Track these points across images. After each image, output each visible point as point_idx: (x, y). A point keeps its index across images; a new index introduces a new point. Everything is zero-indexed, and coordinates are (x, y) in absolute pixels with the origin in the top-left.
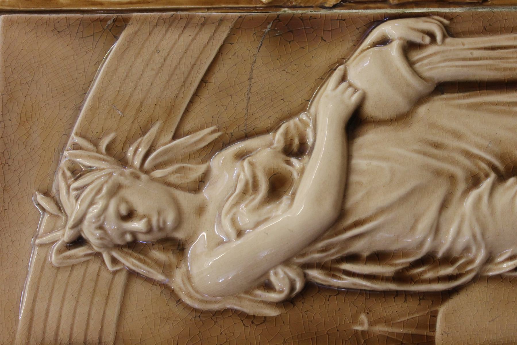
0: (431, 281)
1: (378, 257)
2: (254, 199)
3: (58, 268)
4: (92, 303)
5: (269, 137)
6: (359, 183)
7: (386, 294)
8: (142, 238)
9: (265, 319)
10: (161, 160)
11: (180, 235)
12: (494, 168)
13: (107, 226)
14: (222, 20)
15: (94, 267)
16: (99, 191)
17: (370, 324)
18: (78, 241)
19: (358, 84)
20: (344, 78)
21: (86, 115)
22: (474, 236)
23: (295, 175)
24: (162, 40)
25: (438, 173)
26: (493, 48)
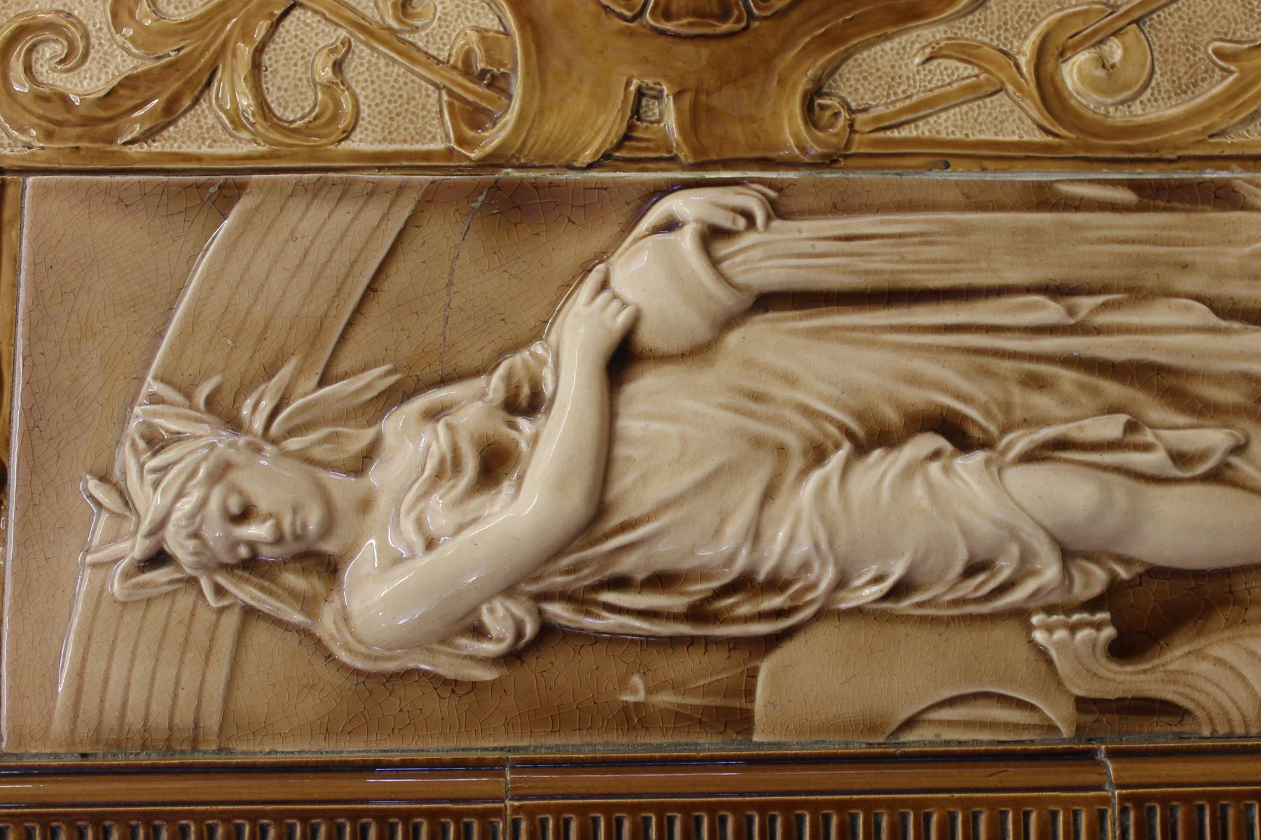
0: (747, 619)
1: (661, 581)
2: (453, 486)
3: (125, 604)
4: (182, 661)
5: (481, 382)
6: (629, 459)
7: (674, 642)
8: (267, 553)
9: (474, 685)
10: (298, 421)
11: (330, 547)
12: (849, 434)
13: (206, 533)
14: (402, 188)
15: (185, 601)
16: (193, 473)
17: (649, 691)
18: (158, 558)
19: (628, 294)
20: (604, 285)
21: (171, 345)
22: (817, 546)
23: (523, 446)
24: (301, 220)
25: (758, 442)
26: (848, 238)
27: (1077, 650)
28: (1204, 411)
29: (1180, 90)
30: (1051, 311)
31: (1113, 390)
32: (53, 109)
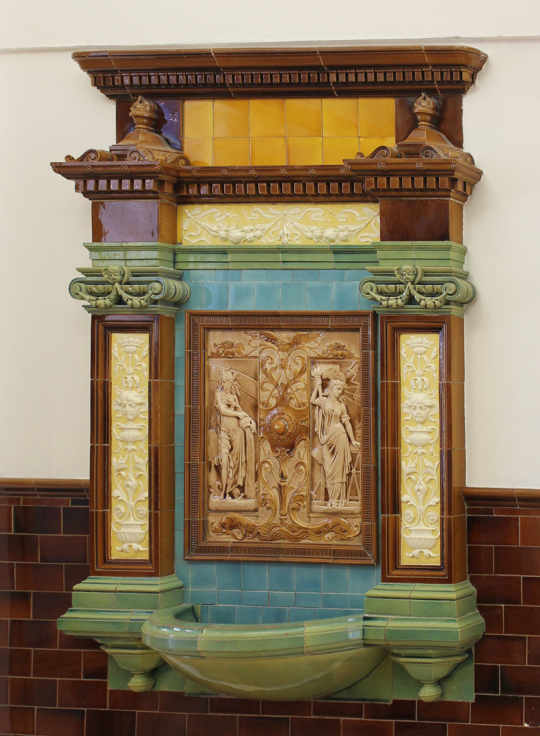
27: (215, 462)
29: (265, 476)
30: (244, 461)
31: (237, 467)
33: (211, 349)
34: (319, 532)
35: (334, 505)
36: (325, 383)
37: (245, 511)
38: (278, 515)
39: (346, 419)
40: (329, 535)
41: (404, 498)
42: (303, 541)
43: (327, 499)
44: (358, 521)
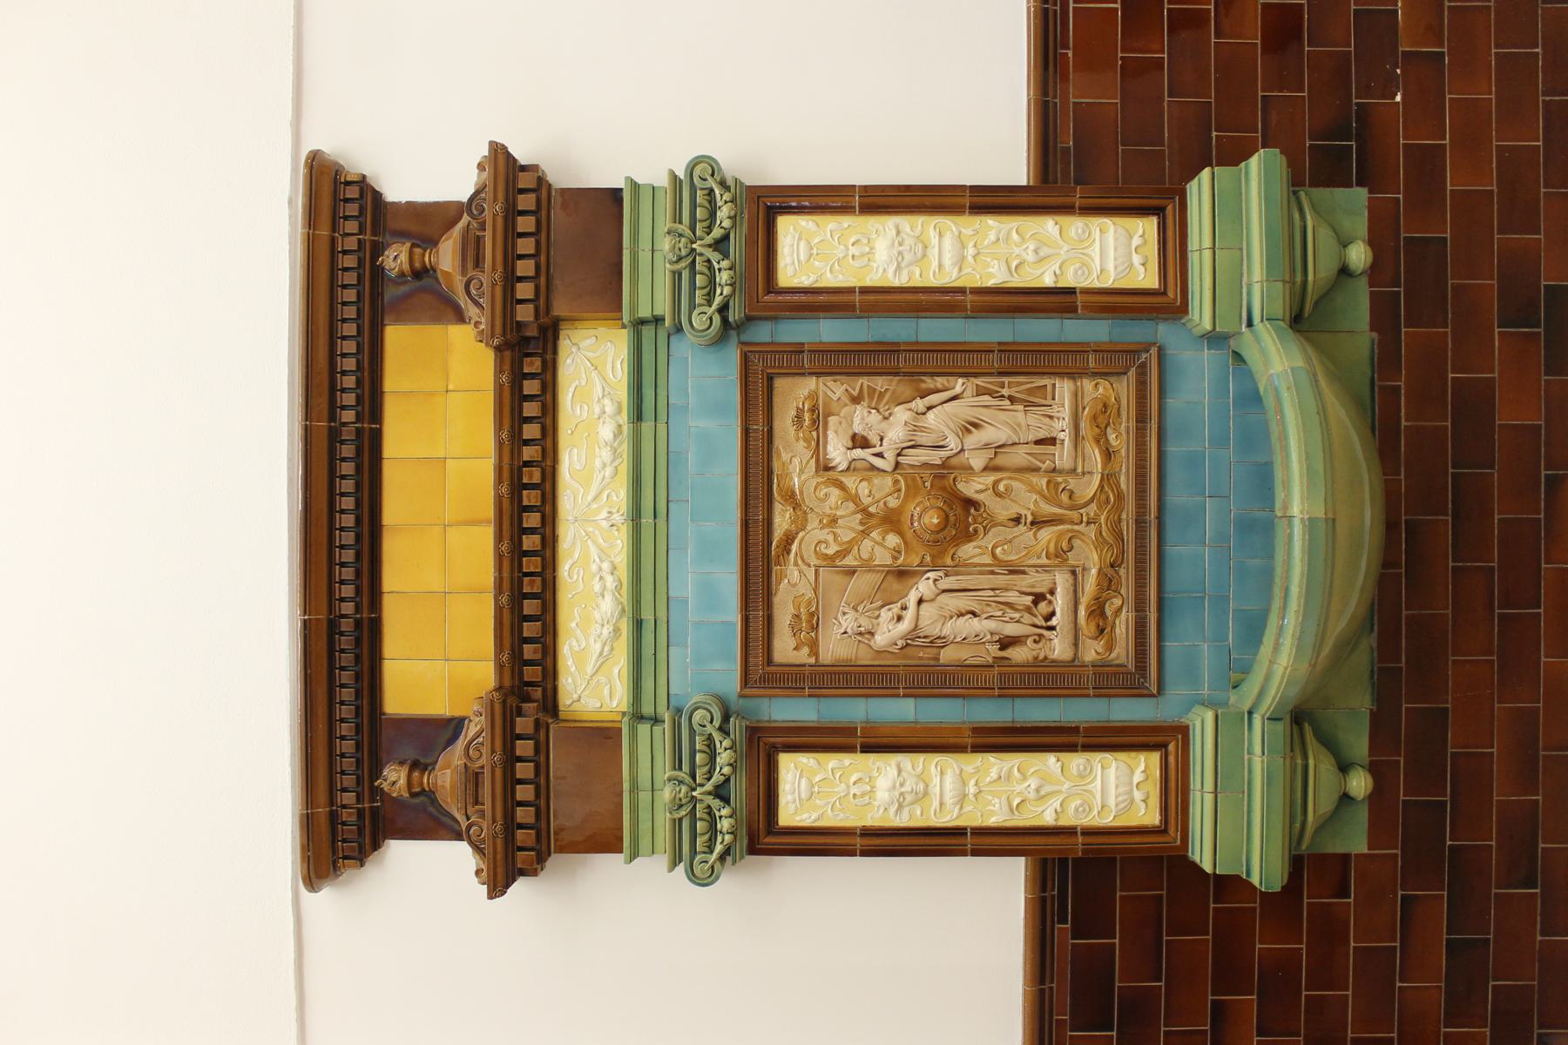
27: (994, 650)
28: (1017, 610)
32: (826, 557)
33: (803, 656)
34: (1108, 454)
35: (1061, 426)
36: (860, 442)
37: (1075, 591)
38: (1081, 528)
39: (920, 404)
40: (1112, 437)
41: (1048, 281)
42: (1123, 486)
43: (1052, 441)
44: (1088, 385)
